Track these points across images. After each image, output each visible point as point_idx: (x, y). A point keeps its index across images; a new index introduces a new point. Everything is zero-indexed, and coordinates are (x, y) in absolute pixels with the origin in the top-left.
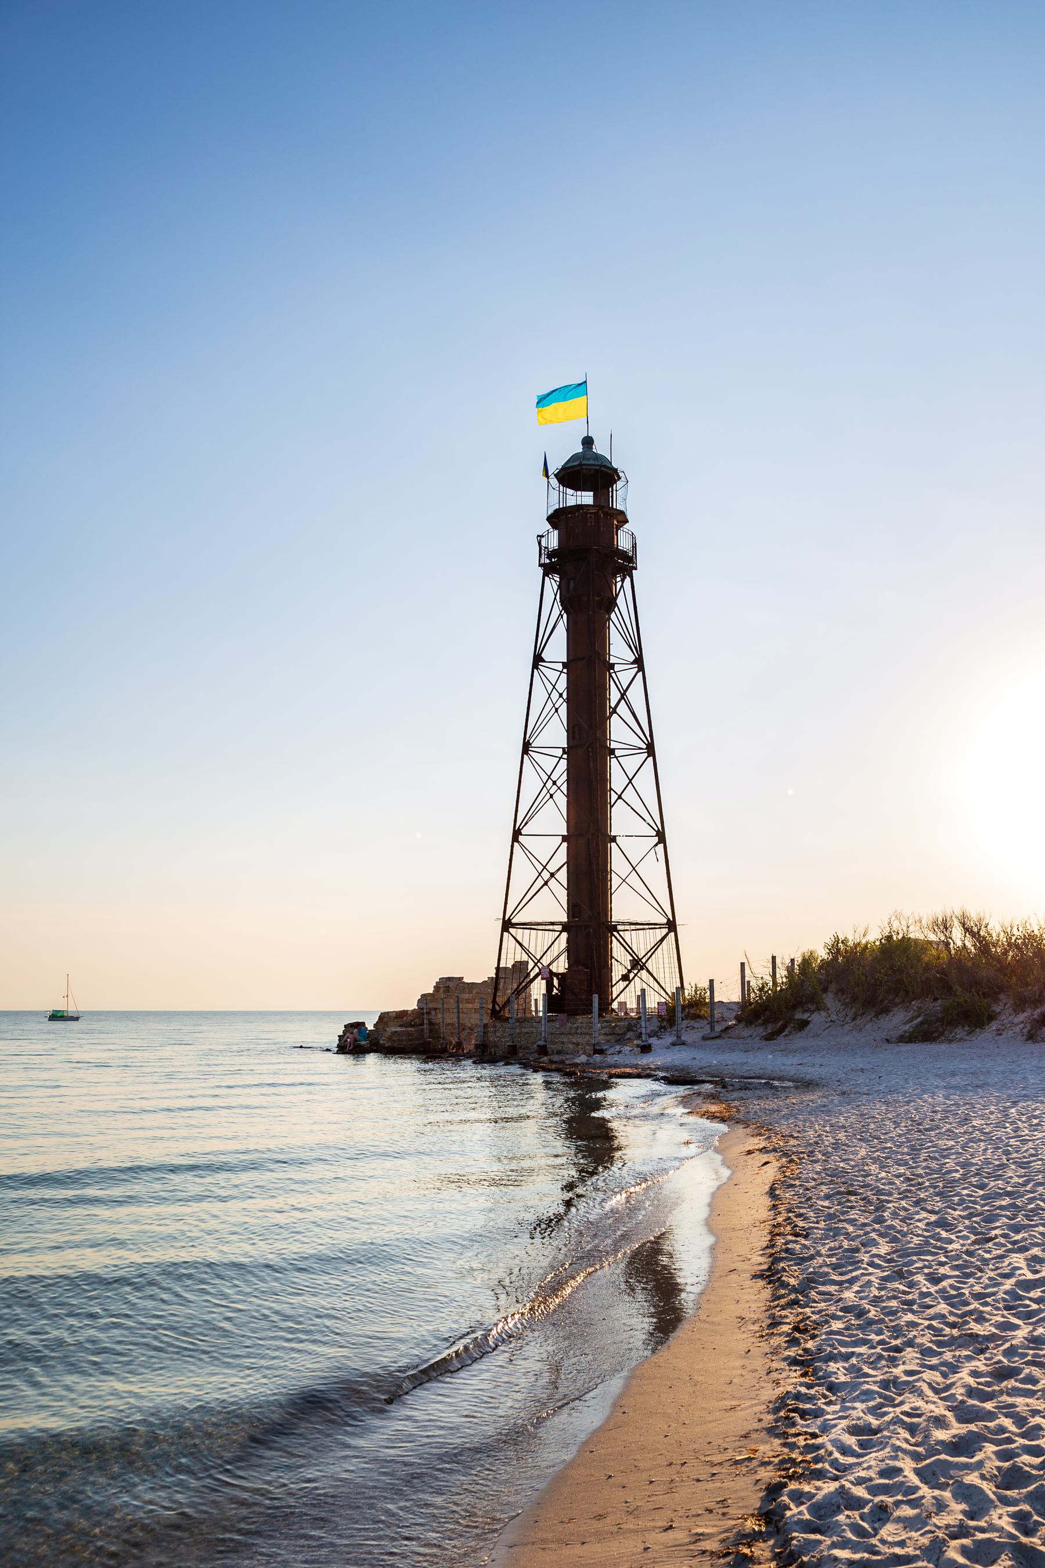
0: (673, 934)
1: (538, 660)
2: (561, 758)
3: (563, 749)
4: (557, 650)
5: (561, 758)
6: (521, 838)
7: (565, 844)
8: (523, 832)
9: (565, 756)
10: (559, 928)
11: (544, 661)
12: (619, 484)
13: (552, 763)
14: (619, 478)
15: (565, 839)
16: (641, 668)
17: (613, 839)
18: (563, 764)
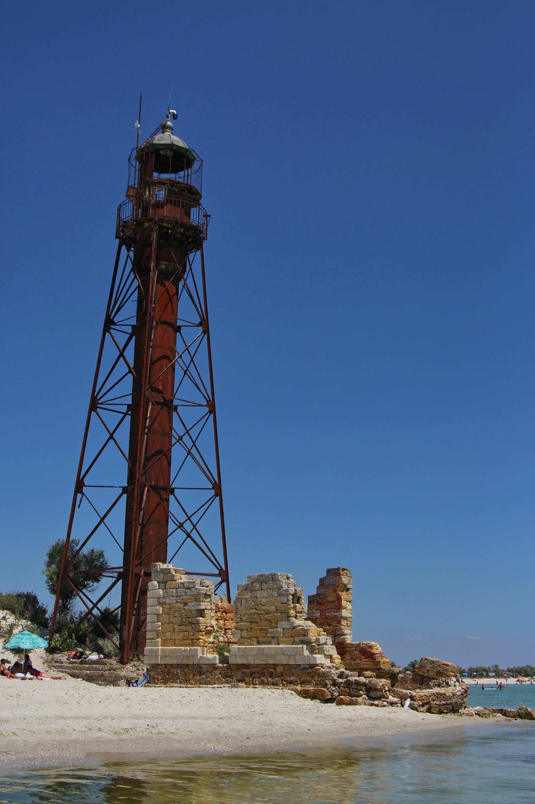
0: (224, 584)
1: (109, 323)
2: (126, 414)
3: (129, 406)
4: (128, 314)
5: (126, 414)
6: (85, 489)
7: (125, 496)
8: (86, 481)
9: (130, 413)
10: (116, 575)
11: (115, 324)
12: (196, 165)
13: (115, 419)
14: (195, 159)
15: (125, 490)
16: (206, 331)
17: (172, 491)
18: (128, 418)
